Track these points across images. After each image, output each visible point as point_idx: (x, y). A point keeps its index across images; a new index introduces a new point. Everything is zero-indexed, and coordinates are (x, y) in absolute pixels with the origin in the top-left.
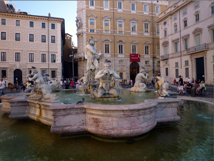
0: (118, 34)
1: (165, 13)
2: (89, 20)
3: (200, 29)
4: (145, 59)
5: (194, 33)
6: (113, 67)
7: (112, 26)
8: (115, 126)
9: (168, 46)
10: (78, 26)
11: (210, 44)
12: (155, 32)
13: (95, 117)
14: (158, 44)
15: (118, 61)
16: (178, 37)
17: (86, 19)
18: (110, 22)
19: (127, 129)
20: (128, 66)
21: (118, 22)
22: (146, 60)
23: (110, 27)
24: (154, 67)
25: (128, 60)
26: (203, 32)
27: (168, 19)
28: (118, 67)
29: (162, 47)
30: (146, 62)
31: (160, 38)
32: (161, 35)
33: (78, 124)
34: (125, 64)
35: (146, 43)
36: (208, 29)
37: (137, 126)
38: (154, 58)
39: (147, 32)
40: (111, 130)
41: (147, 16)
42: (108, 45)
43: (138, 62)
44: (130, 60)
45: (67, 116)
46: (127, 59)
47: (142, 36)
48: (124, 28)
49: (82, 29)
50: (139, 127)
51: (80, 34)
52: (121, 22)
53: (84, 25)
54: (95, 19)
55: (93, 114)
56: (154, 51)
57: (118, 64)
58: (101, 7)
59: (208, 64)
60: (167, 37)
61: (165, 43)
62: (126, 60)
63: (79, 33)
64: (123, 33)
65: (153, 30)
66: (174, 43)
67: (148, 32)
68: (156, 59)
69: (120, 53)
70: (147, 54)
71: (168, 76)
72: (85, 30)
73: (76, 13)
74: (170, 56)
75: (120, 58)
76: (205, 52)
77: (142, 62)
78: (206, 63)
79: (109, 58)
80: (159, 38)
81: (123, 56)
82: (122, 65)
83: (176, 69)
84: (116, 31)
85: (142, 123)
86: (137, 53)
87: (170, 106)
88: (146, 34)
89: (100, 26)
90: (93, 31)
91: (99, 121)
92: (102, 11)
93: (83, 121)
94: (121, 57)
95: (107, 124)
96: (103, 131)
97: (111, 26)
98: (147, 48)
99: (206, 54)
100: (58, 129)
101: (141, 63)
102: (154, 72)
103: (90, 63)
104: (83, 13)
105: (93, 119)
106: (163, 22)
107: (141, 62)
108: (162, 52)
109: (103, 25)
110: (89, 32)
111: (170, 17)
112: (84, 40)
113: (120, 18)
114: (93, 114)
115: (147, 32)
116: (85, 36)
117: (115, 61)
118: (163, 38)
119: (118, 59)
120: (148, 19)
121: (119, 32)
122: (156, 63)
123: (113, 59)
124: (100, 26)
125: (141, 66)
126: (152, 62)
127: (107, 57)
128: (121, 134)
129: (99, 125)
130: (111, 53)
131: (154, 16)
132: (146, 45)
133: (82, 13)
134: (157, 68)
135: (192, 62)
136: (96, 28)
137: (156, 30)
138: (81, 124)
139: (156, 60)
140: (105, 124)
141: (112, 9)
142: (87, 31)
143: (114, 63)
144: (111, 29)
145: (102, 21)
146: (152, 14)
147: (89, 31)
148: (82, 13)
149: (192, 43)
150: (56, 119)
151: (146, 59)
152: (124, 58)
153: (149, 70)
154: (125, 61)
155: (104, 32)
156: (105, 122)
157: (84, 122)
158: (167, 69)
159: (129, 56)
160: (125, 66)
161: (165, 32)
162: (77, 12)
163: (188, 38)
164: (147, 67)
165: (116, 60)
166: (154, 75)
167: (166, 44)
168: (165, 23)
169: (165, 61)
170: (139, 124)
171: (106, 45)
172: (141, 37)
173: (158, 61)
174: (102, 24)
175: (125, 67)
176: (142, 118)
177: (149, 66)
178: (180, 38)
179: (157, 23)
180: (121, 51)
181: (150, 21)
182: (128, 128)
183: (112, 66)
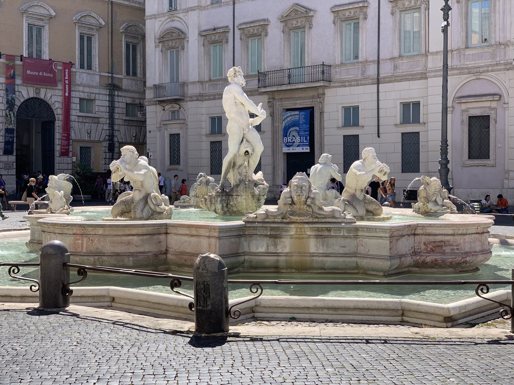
3: (308, 10)
5: (285, 19)
9: (183, 49)
11: (336, 66)
16: (224, 24)
22: (82, 96)
24: (112, 124)
26: (314, 23)
29: (158, 50)
35: (83, 19)
36: (331, 17)
56: (115, 61)
59: (326, 132)
66: (206, 43)
68: (120, 94)
76: (321, 91)
78: (322, 128)
80: (143, 10)
83: (212, 143)
98: (86, 41)
99: (324, 100)
108: (156, 67)
118: (163, 15)
122: (120, 111)
126: (107, 104)
134: (122, 129)
135: (273, 120)
139: (120, 99)
149: (275, 52)
153: (92, 139)
158: (175, 139)
163: (263, 34)
169: (167, 107)
173: (129, 101)
177: (96, 120)
178: (231, 27)
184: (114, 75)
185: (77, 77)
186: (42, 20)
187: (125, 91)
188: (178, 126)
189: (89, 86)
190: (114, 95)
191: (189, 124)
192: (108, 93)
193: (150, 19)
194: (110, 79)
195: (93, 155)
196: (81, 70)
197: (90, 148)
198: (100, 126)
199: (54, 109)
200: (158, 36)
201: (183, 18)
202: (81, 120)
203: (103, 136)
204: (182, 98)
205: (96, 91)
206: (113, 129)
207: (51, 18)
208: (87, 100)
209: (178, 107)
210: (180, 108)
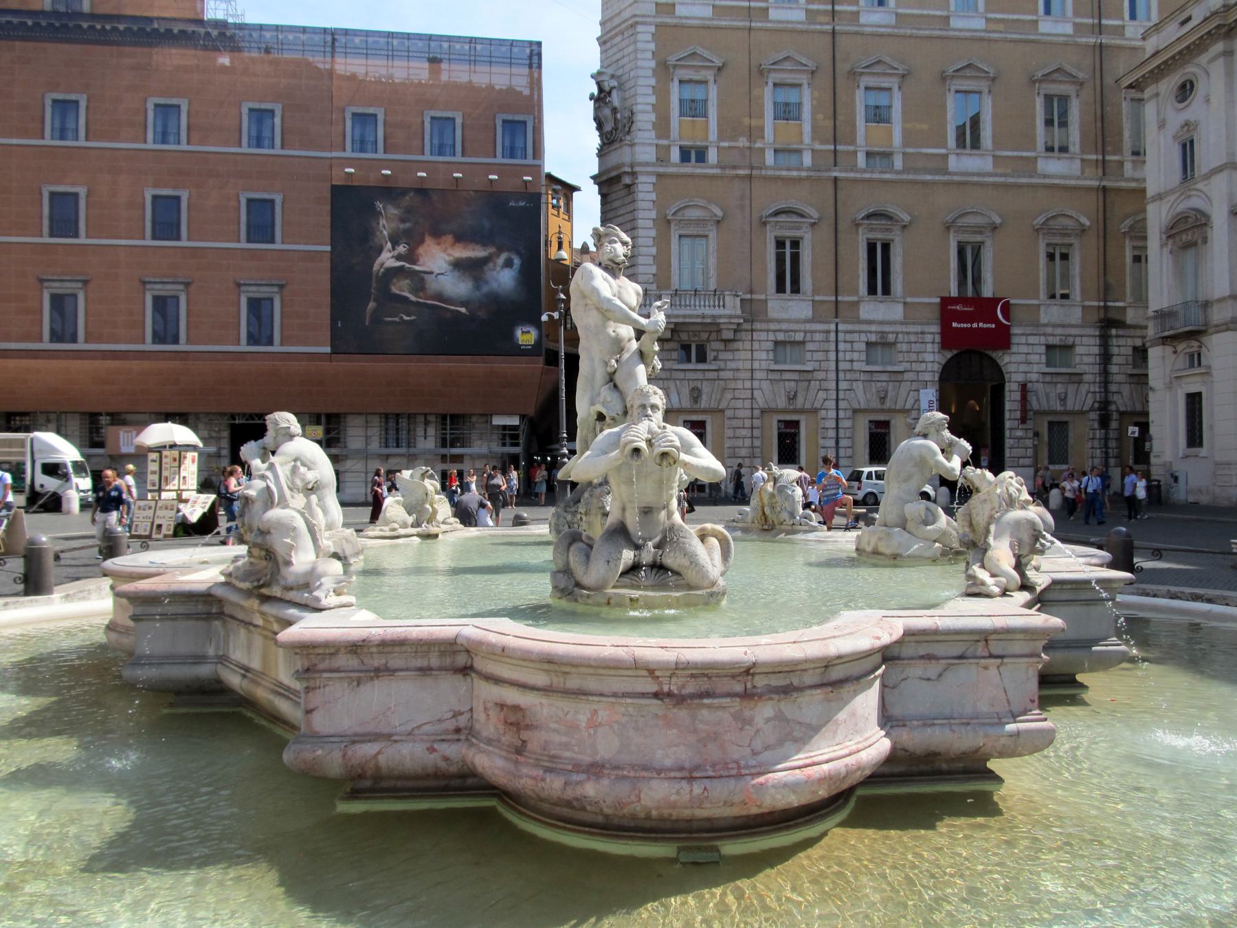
0: (864, 171)
1: (1189, 19)
2: (675, 88)
4: (1041, 330)
6: (825, 385)
7: (820, 116)
8: (607, 756)
9: (1205, 241)
10: (608, 127)
12: (1118, 150)
13: (512, 696)
14: (1139, 233)
15: (863, 347)
17: (653, 82)
18: (806, 92)
19: (673, 774)
20: (928, 377)
21: (860, 94)
22: (1051, 341)
23: (807, 128)
25: (929, 338)
27: (1203, 59)
28: (858, 387)
29: (1166, 250)
30: (1049, 347)
31: (1150, 193)
32: (1158, 170)
33: (427, 728)
34: (907, 366)
35: (1051, 223)
37: (737, 762)
38: (1109, 324)
39: (1064, 149)
40: (583, 776)
41: (1066, 44)
42: (795, 244)
43: (994, 355)
44: (938, 338)
45: (369, 685)
46: (918, 328)
47: (1024, 180)
48: (906, 134)
49: (632, 145)
50: (747, 767)
51: (618, 178)
52: (884, 95)
53: (645, 119)
54: (711, 79)
55: (498, 681)
56: (1111, 279)
57: (856, 366)
58: (753, 4)
60: (1200, 186)
61: (1183, 227)
62: (912, 338)
63: (609, 171)
64: (898, 163)
65: (1104, 136)
67: (1071, 148)
68: (1121, 332)
69: (872, 290)
70: (1058, 301)
71: (1203, 452)
72: (645, 154)
73: (598, 49)
74: (1219, 315)
75: (873, 328)
77: (1024, 349)
79: (802, 327)
80: (1144, 191)
81: (895, 311)
82: (890, 368)
84: (848, 152)
85: (767, 748)
86: (987, 292)
87: (991, 656)
88: (1054, 168)
89: (746, 121)
90: (701, 156)
91: (528, 721)
92: (759, 25)
93: (454, 716)
94: (879, 316)
95: (564, 739)
96: (543, 780)
97: (814, 119)
98: (1058, 256)
100: (319, 752)
101: (1014, 358)
102: (1104, 422)
103: (593, 376)
104: (640, 45)
105: (502, 706)
106: (1168, 85)
107: (1014, 349)
109: (762, 116)
110: (675, 165)
111: (1219, 47)
112: (641, 214)
113: (877, 69)
114: (498, 681)
115: (1064, 149)
116: (646, 190)
117: (842, 346)
118: (1171, 192)
119: (860, 332)
120: (1068, 68)
121: (869, 155)
123: (828, 332)
124: (746, 121)
125: (1015, 377)
126: (1096, 350)
127: (785, 316)
128: (633, 798)
129: (529, 746)
130: (816, 291)
131: (1108, 46)
132: (1057, 240)
133: (631, 48)
134: (1126, 390)
136: (721, 137)
137: (1127, 134)
138: (446, 732)
139: (1122, 342)
140: (557, 738)
141: (825, 12)
142: (662, 159)
143: (832, 356)
144: (813, 139)
145: (755, 92)
146: (1100, 29)
147: (675, 155)
148: (631, 48)
150: (316, 699)
151: (1049, 330)
152: (898, 328)
153: (1070, 407)
154: (904, 347)
155: (769, 158)
156: (555, 731)
157: (462, 721)
158: (1194, 402)
159: (936, 314)
160: (907, 376)
161: (1187, 149)
162: (602, 41)
164: (1060, 388)
165: (849, 337)
166: (1106, 439)
167: (1189, 232)
168: (1183, 86)
169: (1181, 347)
170: (748, 750)
171: (780, 244)
172: (1021, 186)
173: (1138, 343)
174: (754, 109)
175: (905, 387)
176: (768, 720)
177: (1076, 378)
179: (1130, 86)
180: (879, 281)
181: (1081, 75)
182: (681, 769)
183: (821, 375)
184: (1110, 304)
185: (1042, 315)
186: (981, 233)
187: (1130, 327)
188: (1198, 379)
189: (1063, 326)
190: (1110, 336)
191: (1215, 373)
192: (1097, 333)
193: (1154, 201)
194: (1102, 311)
195: (1071, 435)
196: (1053, 301)
197: (1066, 423)
198: (1084, 388)
199: (1001, 364)
200: (1164, 229)
201: (1205, 189)
202: (1048, 379)
203: (1089, 402)
204: (1202, 328)
205: (1073, 331)
206: (1106, 391)
207: (995, 228)
208: (1061, 347)
209: (1195, 344)
210: (1200, 347)
